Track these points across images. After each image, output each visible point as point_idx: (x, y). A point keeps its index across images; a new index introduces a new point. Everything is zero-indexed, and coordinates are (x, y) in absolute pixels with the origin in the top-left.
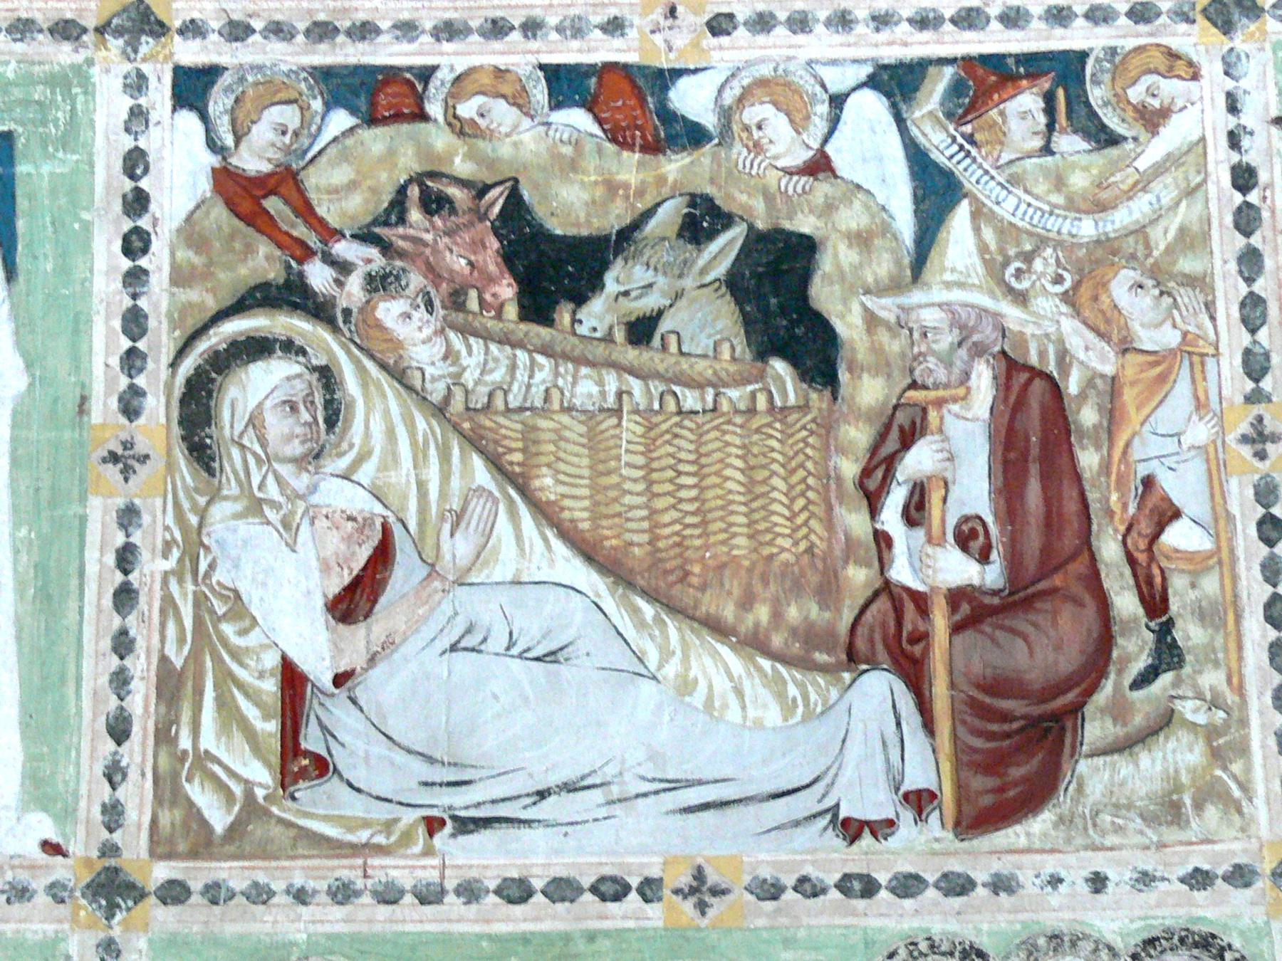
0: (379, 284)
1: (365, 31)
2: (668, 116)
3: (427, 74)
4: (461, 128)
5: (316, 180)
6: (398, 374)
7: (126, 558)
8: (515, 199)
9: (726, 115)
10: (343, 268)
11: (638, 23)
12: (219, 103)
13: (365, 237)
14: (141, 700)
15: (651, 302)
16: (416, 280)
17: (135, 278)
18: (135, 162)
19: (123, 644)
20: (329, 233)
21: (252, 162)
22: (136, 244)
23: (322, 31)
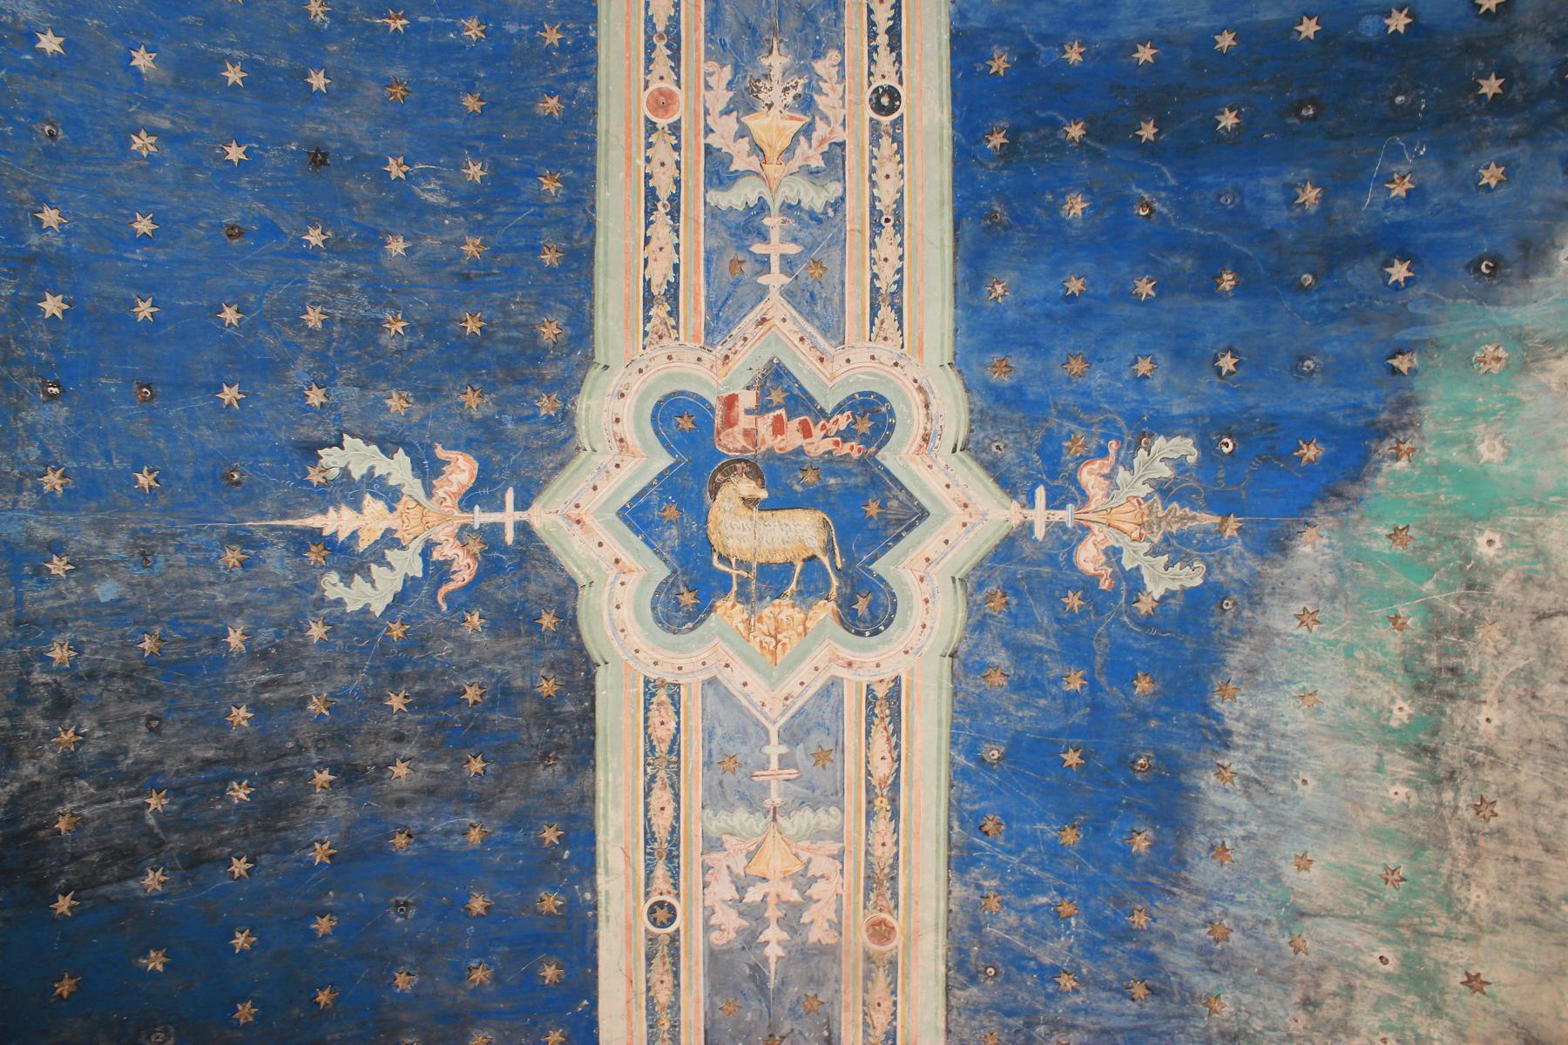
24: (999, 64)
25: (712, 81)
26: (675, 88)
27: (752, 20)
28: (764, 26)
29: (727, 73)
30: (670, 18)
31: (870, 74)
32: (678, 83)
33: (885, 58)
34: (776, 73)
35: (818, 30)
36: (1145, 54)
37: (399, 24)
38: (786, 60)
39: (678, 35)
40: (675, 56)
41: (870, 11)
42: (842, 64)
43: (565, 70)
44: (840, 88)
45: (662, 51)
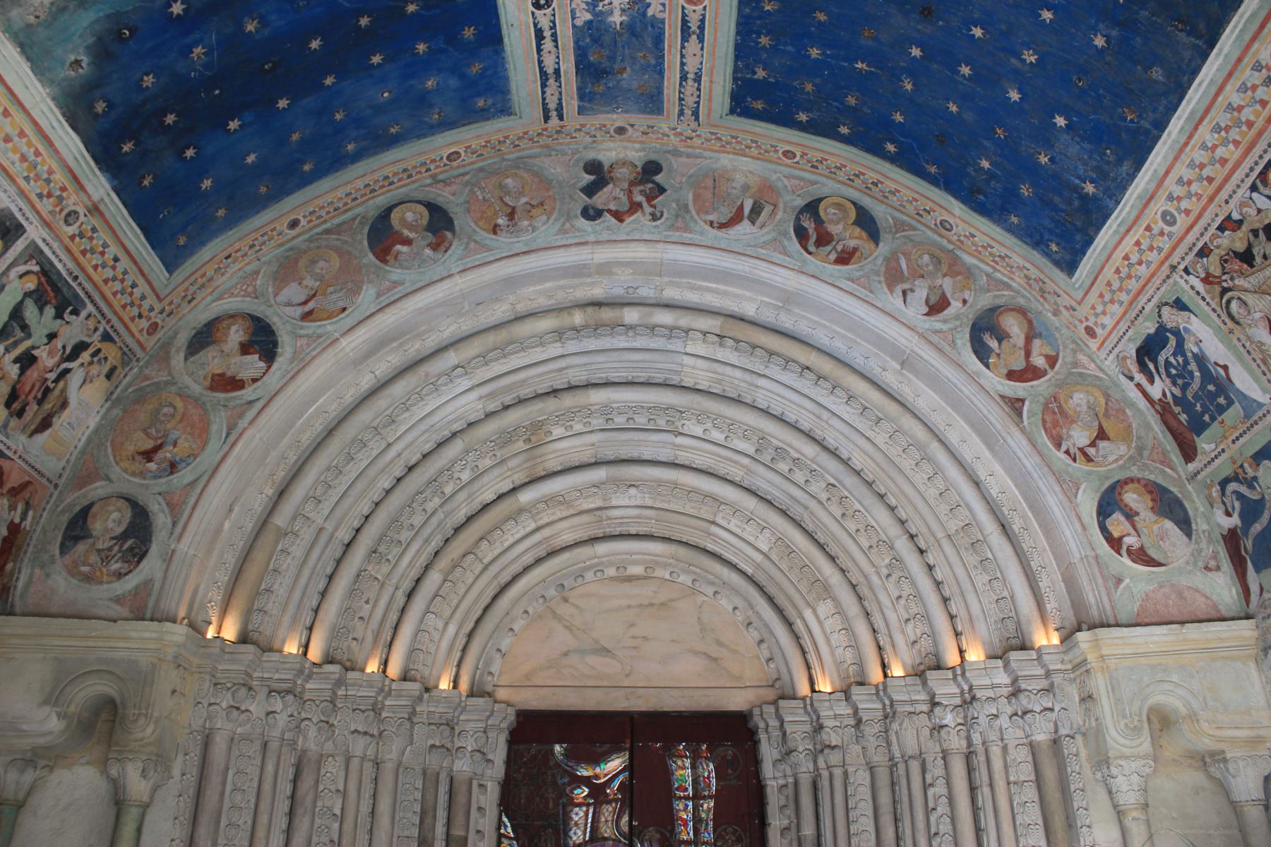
0: (1232, 279)
1: (1194, 245)
2: (1236, 221)
3: (1206, 243)
4: (1218, 247)
5: (1211, 270)
6: (1246, 290)
7: (1244, 346)
8: (1234, 252)
9: (1241, 214)
10: (1226, 281)
11: (1218, 211)
12: (1191, 271)
13: (1224, 274)
14: (1263, 368)
15: (1262, 253)
16: (1235, 275)
17: (1208, 303)
18: (1192, 287)
19: (1254, 360)
20: (1220, 277)
21: (1203, 275)
22: (1203, 299)
23: (1190, 249)
24: (469, 33)
25: (661, 8)
26: (686, 5)
27: (634, 39)
28: (625, 37)
29: (650, 12)
30: (688, 41)
31: (554, 15)
32: (683, 8)
33: (545, 23)
34: (617, 13)
35: (590, 35)
36: (376, 59)
37: (859, 65)
38: (611, 19)
39: (682, 33)
40: (685, 22)
41: (557, 47)
42: (573, 18)
43: (758, 22)
44: (574, 6)
45: (694, 26)
